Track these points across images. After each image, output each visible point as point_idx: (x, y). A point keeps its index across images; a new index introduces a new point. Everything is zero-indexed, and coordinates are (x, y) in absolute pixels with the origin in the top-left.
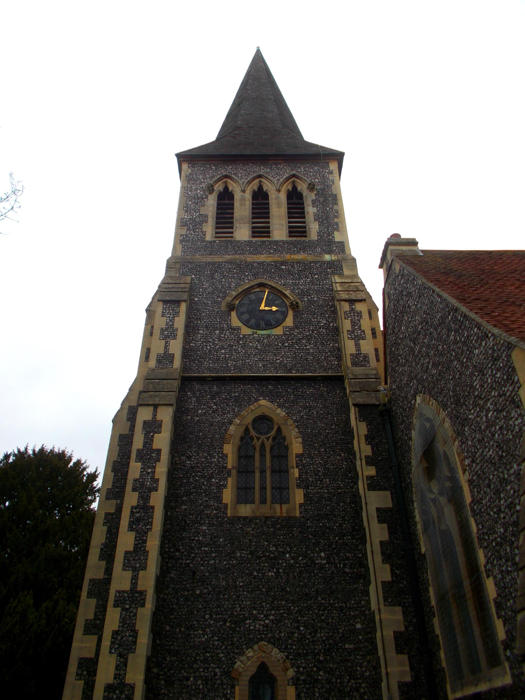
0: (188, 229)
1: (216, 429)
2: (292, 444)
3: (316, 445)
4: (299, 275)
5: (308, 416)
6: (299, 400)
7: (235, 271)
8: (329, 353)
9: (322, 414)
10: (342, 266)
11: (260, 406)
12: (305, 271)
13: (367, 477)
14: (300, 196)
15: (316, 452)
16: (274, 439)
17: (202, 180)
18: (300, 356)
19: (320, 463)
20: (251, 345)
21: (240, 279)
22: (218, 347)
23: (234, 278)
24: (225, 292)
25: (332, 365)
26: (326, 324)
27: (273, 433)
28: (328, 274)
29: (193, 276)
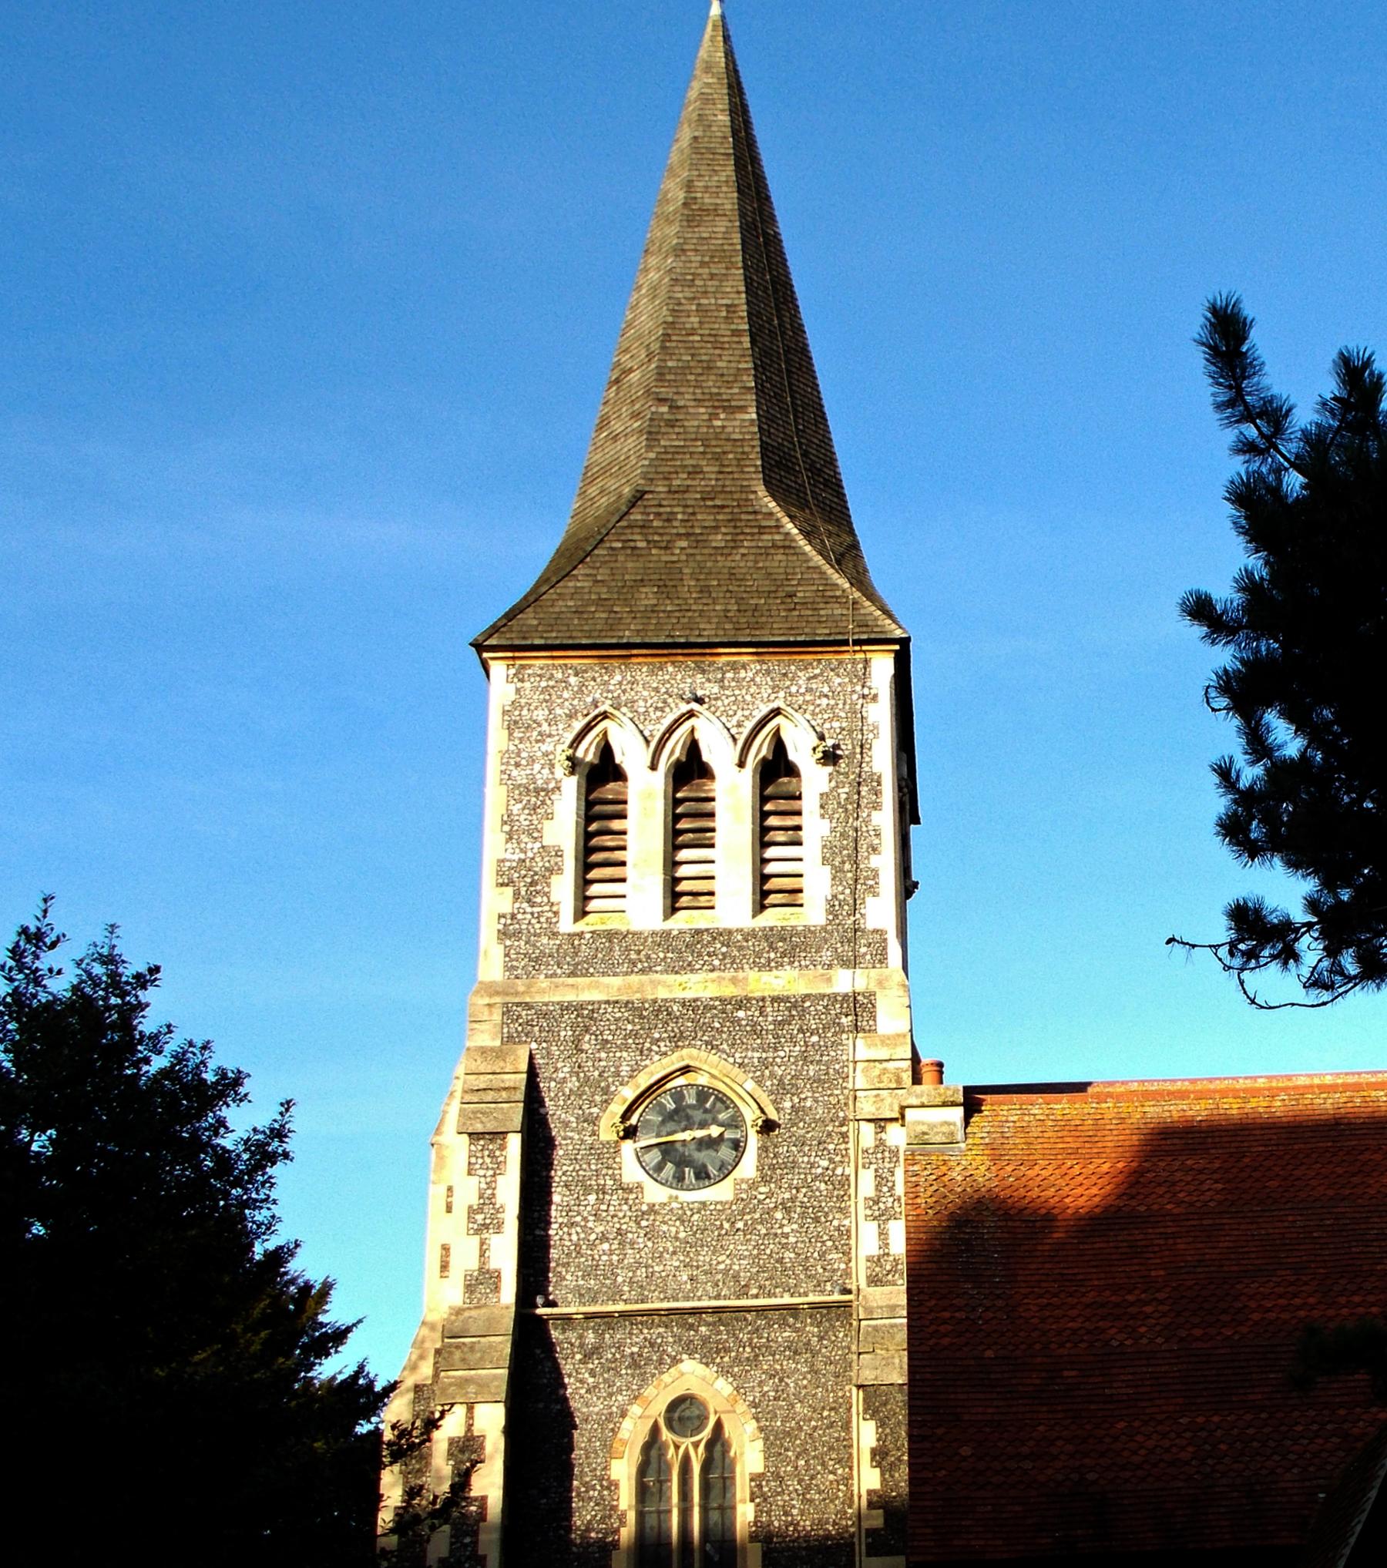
0: (517, 896)
1: (596, 1430)
2: (742, 1454)
3: (790, 1454)
4: (777, 1037)
5: (777, 1391)
6: (761, 1358)
7: (630, 1027)
8: (829, 1243)
9: (805, 1387)
10: (874, 1007)
11: (682, 1374)
12: (790, 1024)
13: (867, 1530)
14: (792, 771)
15: (789, 1468)
16: (710, 1445)
17: (545, 727)
18: (768, 1252)
19: (796, 1490)
20: (665, 1228)
21: (641, 1052)
22: (593, 1237)
23: (627, 1047)
24: (606, 1091)
25: (834, 1271)
26: (827, 1169)
27: (706, 1433)
28: (843, 1032)
29: (534, 1046)
